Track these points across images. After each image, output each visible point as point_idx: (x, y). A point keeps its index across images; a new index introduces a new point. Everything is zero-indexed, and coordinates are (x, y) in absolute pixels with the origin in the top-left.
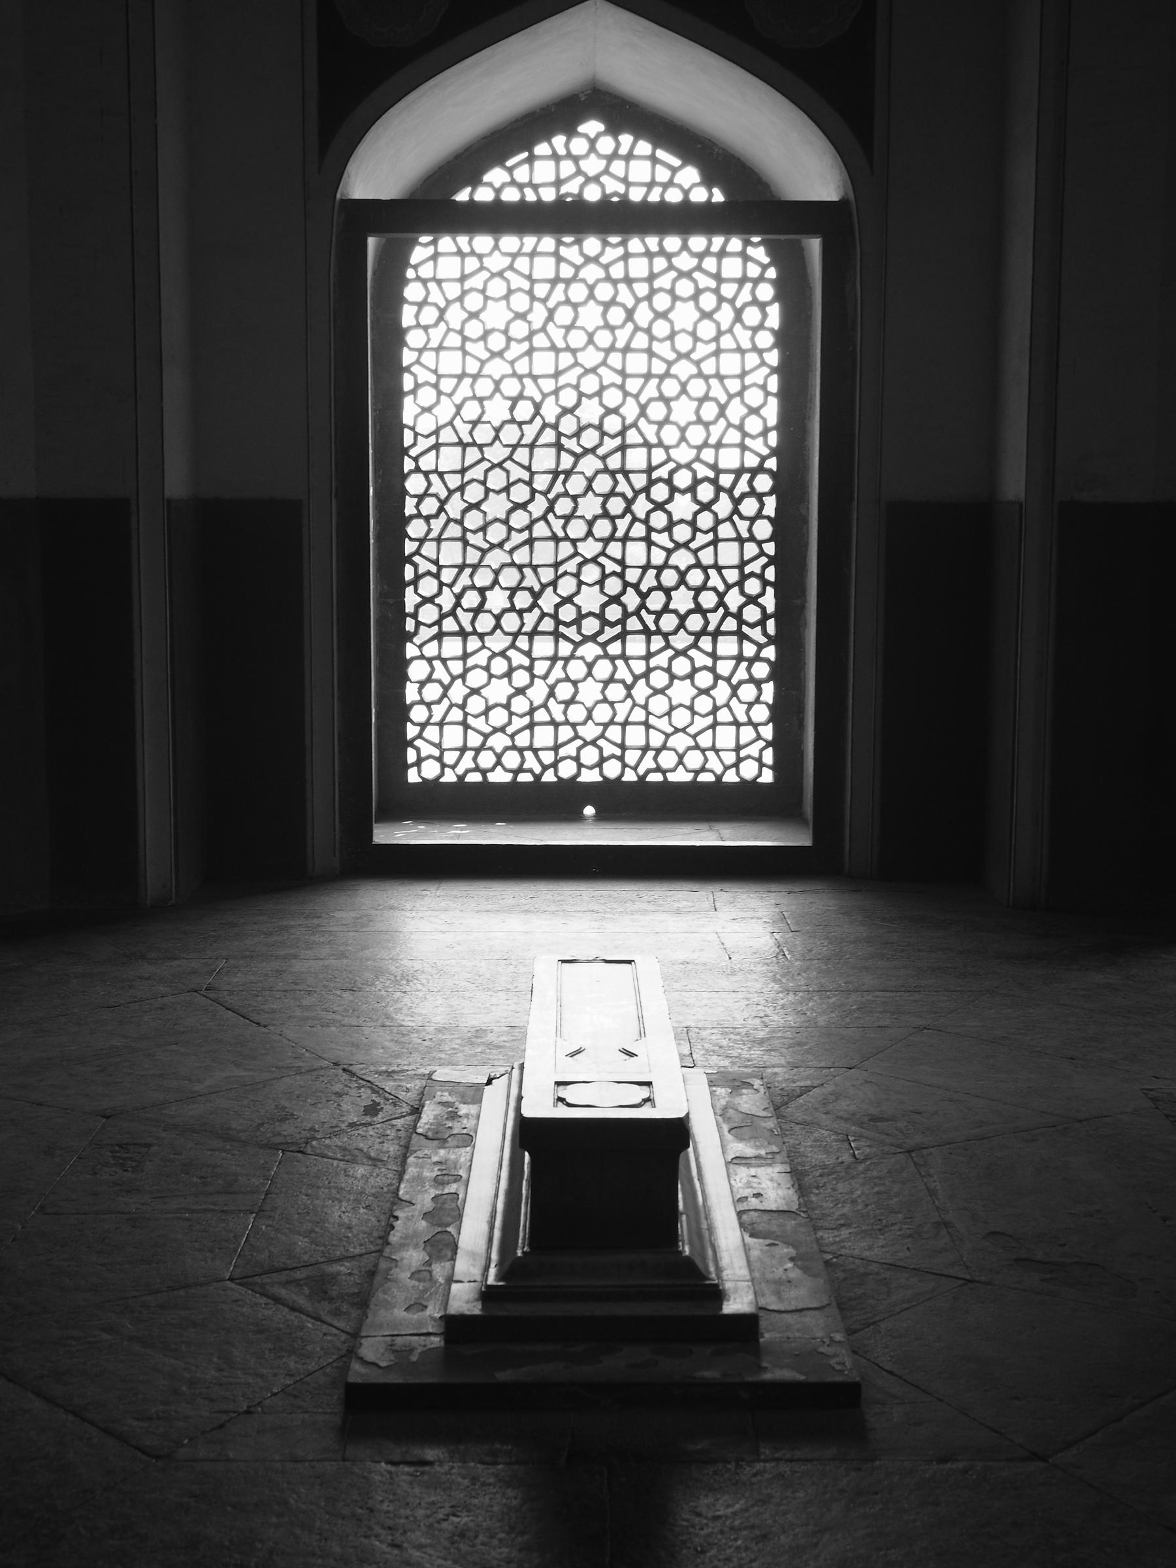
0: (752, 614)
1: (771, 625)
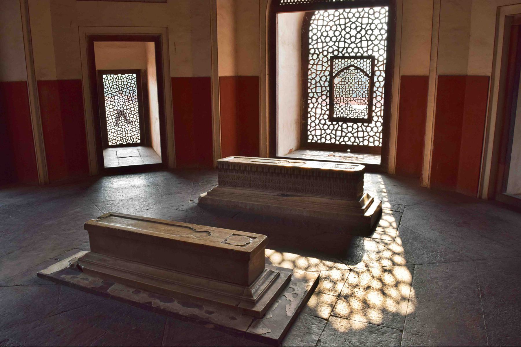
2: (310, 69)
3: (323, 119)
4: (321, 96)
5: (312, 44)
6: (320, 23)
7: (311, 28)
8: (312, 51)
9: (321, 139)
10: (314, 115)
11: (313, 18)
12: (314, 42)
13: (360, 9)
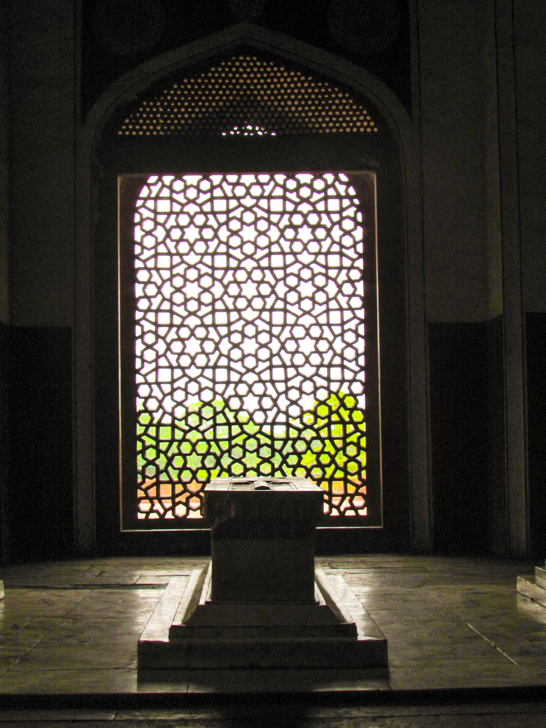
0: (350, 353)
1: (362, 361)
2: (138, 323)
3: (180, 453)
4: (171, 394)
5: (143, 257)
6: (164, 206)
7: (137, 218)
8: (142, 276)
9: (173, 509)
10: (154, 443)
11: (144, 193)
12: (147, 254)
13: (264, 178)
